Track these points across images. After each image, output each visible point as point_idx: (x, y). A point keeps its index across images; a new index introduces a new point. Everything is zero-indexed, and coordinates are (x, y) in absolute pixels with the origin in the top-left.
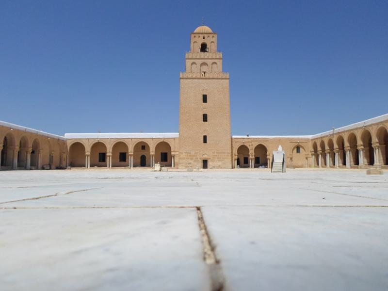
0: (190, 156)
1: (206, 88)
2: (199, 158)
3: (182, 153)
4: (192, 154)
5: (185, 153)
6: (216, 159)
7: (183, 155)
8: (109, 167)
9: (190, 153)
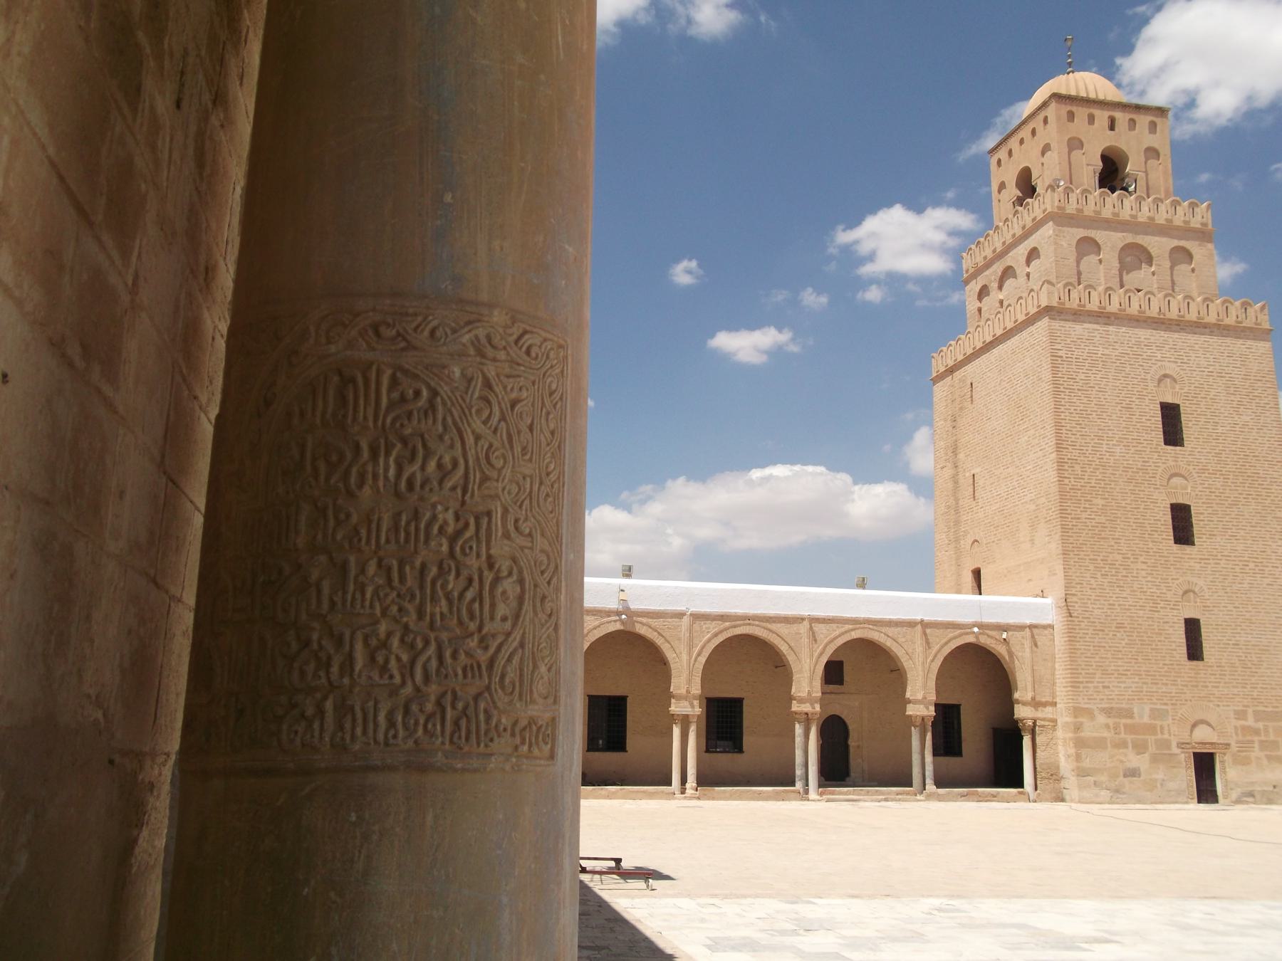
0: (1131, 729)
1: (1171, 369)
2: (1174, 744)
3: (1090, 714)
4: (1137, 720)
5: (1108, 712)
6: (1256, 752)
7: (1096, 727)
8: (684, 780)
9: (1129, 714)
